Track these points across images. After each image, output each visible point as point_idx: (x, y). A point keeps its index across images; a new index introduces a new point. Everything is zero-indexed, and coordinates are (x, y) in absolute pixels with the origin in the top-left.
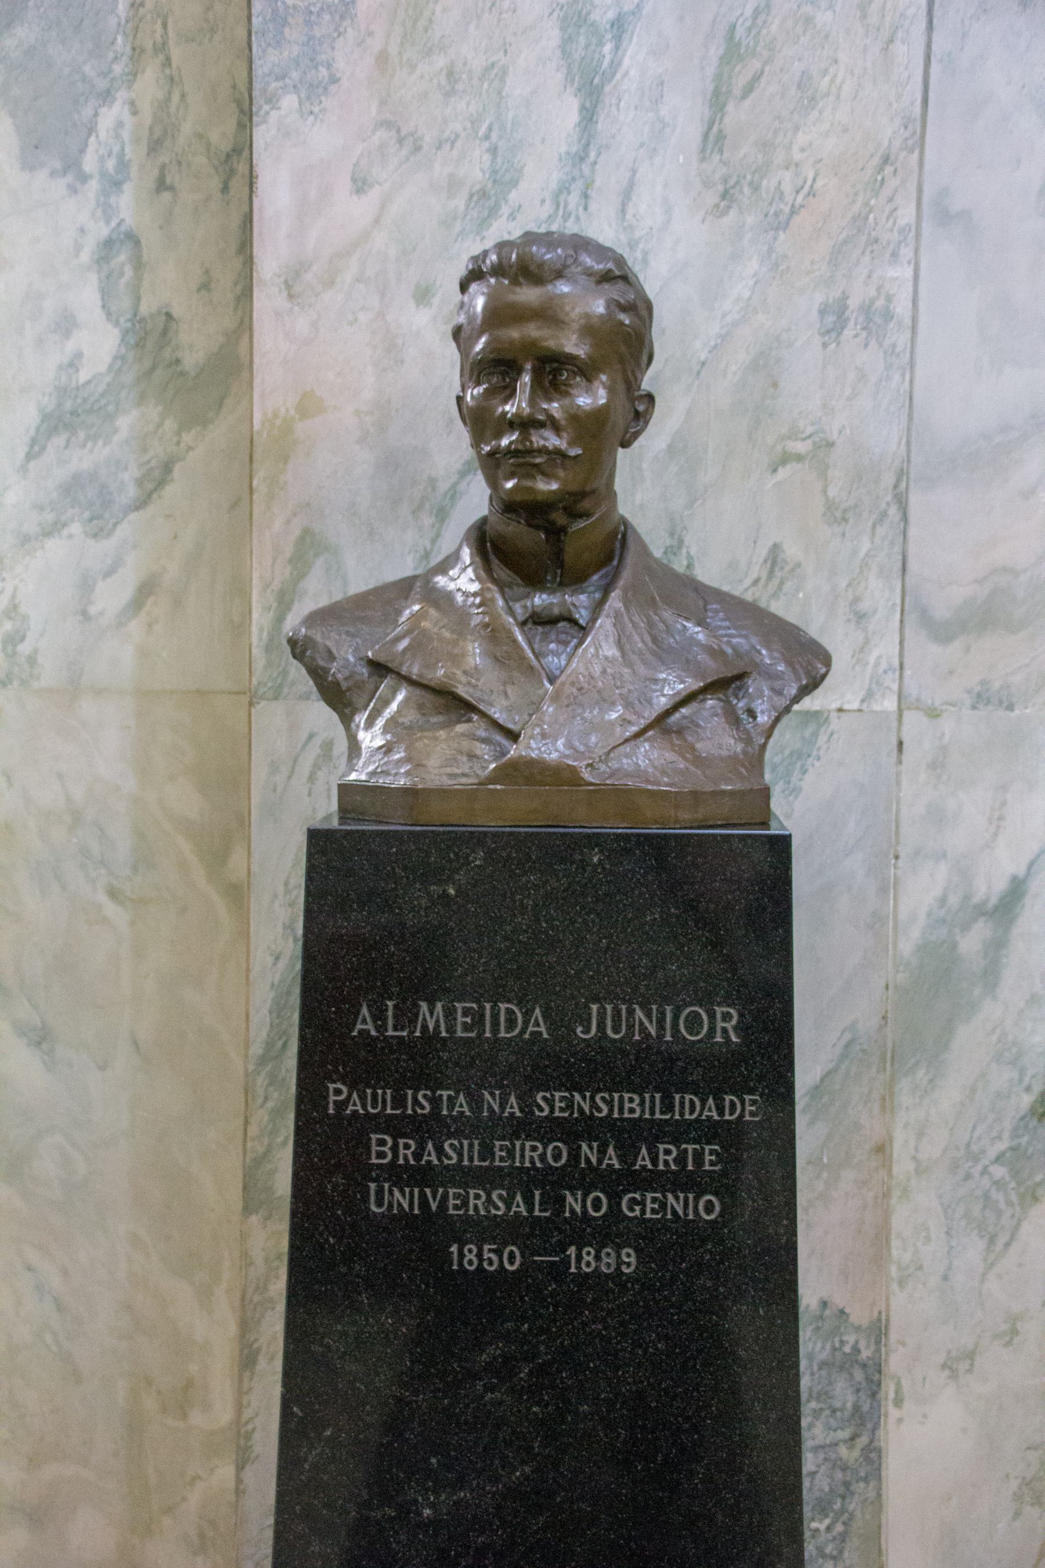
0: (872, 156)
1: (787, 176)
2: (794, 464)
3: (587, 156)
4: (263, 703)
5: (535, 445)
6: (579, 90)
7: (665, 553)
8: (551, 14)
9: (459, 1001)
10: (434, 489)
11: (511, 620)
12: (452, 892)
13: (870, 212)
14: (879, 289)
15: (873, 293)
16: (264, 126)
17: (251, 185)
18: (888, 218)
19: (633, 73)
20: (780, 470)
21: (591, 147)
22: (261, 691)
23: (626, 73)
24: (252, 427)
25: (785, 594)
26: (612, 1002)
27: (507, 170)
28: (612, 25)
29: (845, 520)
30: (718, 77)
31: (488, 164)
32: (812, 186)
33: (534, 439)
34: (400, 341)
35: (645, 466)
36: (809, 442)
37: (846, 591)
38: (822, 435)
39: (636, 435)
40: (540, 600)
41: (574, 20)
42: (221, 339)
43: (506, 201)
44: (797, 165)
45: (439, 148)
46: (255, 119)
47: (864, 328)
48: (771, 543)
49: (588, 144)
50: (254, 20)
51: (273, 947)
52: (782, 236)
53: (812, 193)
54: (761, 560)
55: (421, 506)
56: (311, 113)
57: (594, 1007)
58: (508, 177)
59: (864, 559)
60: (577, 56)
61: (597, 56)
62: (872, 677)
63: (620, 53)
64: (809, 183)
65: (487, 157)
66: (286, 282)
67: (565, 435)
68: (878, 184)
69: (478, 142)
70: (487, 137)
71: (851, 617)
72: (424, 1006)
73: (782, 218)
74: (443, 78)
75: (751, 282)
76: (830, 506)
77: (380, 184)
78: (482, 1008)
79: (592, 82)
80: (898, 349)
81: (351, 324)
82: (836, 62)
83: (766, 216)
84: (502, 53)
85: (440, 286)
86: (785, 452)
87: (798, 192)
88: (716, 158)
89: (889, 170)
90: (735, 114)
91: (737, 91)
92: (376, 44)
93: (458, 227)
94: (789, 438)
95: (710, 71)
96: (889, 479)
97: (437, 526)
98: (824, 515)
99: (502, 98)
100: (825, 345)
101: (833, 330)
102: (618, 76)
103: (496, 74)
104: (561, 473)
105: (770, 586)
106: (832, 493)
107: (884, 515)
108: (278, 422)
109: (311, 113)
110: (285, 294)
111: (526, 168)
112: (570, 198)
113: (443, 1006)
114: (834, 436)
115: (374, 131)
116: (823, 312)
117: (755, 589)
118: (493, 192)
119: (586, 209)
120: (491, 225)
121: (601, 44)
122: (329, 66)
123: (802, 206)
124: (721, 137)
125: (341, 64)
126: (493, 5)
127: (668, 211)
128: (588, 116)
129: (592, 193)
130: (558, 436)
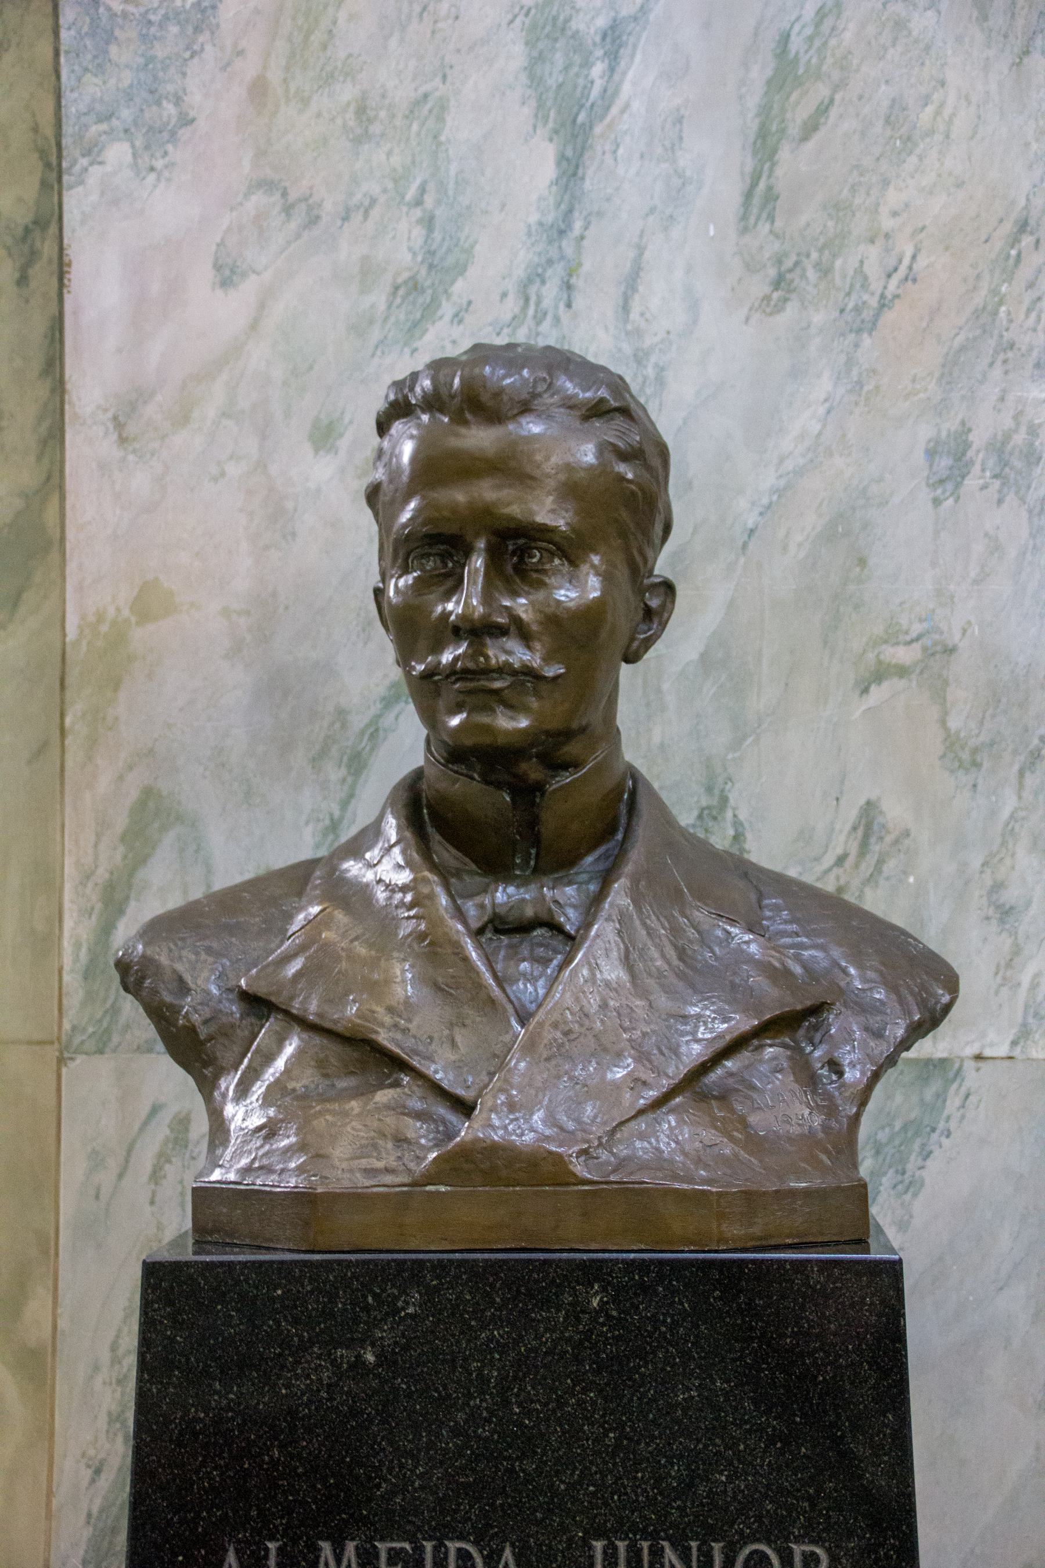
0: (1001, 221)
1: (873, 252)
2: (895, 680)
3: (570, 226)
4: (80, 1059)
5: (494, 661)
6: (556, 132)
7: (700, 817)
8: (511, 22)
9: (382, 1539)
10: (344, 726)
11: (460, 927)
12: (370, 1358)
13: (1001, 303)
14: (1017, 417)
15: (1008, 423)
16: (80, 189)
17: (61, 279)
18: (1029, 311)
19: (636, 105)
20: (873, 688)
21: (576, 214)
22: (76, 1041)
23: (627, 106)
24: (64, 635)
25: (887, 879)
26: (627, 1537)
27: (449, 250)
28: (604, 37)
29: (976, 765)
30: (765, 111)
31: (420, 241)
32: (910, 268)
33: (490, 653)
34: (290, 505)
35: (666, 686)
36: (917, 646)
38: (937, 637)
39: (648, 643)
40: (504, 895)
41: (547, 30)
42: (18, 503)
44: (887, 236)
45: (346, 219)
46: (65, 178)
47: (995, 476)
48: (862, 801)
49: (570, 211)
50: (64, 34)
51: (91, 1452)
52: (867, 341)
53: (911, 278)
54: (848, 827)
55: (324, 752)
56: (152, 169)
57: (598, 1545)
58: (450, 260)
60: (551, 82)
61: (581, 81)
62: (1027, 1007)
63: (616, 77)
64: (906, 261)
65: (418, 233)
66: (115, 418)
67: (538, 645)
68: (1011, 261)
69: (405, 209)
70: (418, 202)
71: (991, 912)
72: (326, 1548)
73: (868, 315)
74: (350, 115)
75: (821, 410)
76: (952, 743)
77: (258, 274)
78: (419, 1549)
79: (574, 121)
81: (215, 480)
82: (943, 84)
83: (842, 311)
84: (438, 79)
85: (351, 422)
86: (880, 662)
87: (889, 276)
88: (764, 228)
89: (1027, 241)
90: (792, 163)
91: (794, 130)
92: (249, 68)
94: (886, 642)
95: (753, 101)
97: (350, 779)
98: (943, 756)
99: (439, 144)
100: (937, 502)
102: (614, 110)
103: (430, 108)
104: (534, 703)
105: (863, 866)
106: (954, 723)
108: (104, 628)
109: (152, 169)
110: (114, 437)
111: (478, 247)
112: (544, 290)
113: (357, 1548)
115: (247, 196)
116: (931, 453)
117: (841, 870)
118: (428, 283)
119: (569, 305)
120: (427, 330)
121: (587, 64)
122: (178, 101)
123: (897, 296)
124: (771, 197)
125: (195, 98)
126: (424, 9)
127: (694, 307)
128: (571, 171)
129: (576, 281)
130: (529, 647)
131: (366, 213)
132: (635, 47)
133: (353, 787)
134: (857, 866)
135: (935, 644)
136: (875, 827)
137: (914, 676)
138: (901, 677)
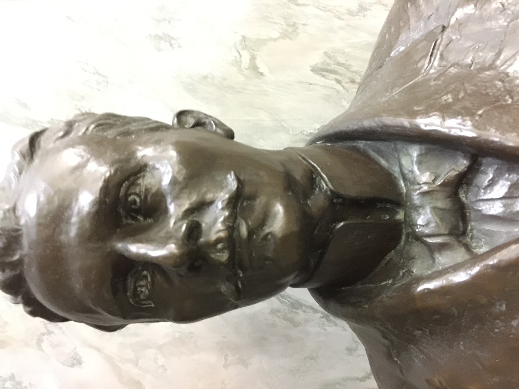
2: (257, 61)
5: (222, 234)
10: (279, 311)
20: (260, 70)
29: (295, 23)
33: (213, 237)
34: (177, 335)
36: (242, 52)
39: (219, 124)
48: (311, 73)
54: (323, 79)
55: (291, 321)
67: (209, 196)
71: (362, 15)
76: (285, 35)
77: (76, 347)
86: (249, 68)
94: (240, 66)
97: (304, 308)
98: (290, 39)
105: (340, 71)
106: (275, 35)
115: (43, 351)
117: (343, 82)
122: (5, 381)
130: (211, 203)
133: (307, 307)
134: (341, 75)
135: (241, 44)
136: (323, 67)
137: (255, 53)
138: (255, 59)
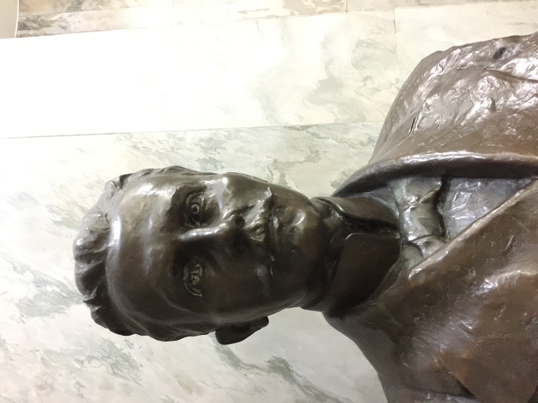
0: (131, 153)
2: (286, 178)
8: (24, 323)
14: (196, 145)
15: (198, 147)
18: (161, 143)
28: (38, 286)
29: (317, 151)
33: (253, 224)
36: (273, 172)
37: (356, 148)
38: (270, 166)
43: (122, 349)
45: (82, 396)
47: (215, 150)
58: (107, 349)
59: (339, 142)
63: (53, 281)
65: (95, 363)
68: (145, 149)
69: (83, 369)
70: (82, 362)
74: (42, 392)
76: (309, 159)
80: (227, 134)
85: (167, 396)
89: (139, 145)
93: (132, 384)
96: (294, 133)
98: (315, 162)
101: (215, 164)
104: (288, 209)
107: (313, 134)
111: (104, 337)
114: (271, 160)
118: (114, 359)
120: (134, 360)
121: (46, 293)
131: (82, 386)
132: (45, 275)
135: (273, 166)
137: (284, 172)
138: (285, 176)
